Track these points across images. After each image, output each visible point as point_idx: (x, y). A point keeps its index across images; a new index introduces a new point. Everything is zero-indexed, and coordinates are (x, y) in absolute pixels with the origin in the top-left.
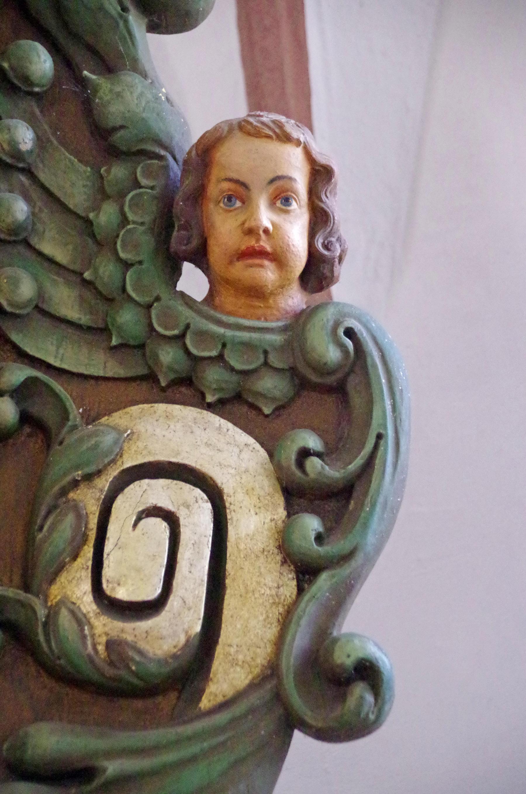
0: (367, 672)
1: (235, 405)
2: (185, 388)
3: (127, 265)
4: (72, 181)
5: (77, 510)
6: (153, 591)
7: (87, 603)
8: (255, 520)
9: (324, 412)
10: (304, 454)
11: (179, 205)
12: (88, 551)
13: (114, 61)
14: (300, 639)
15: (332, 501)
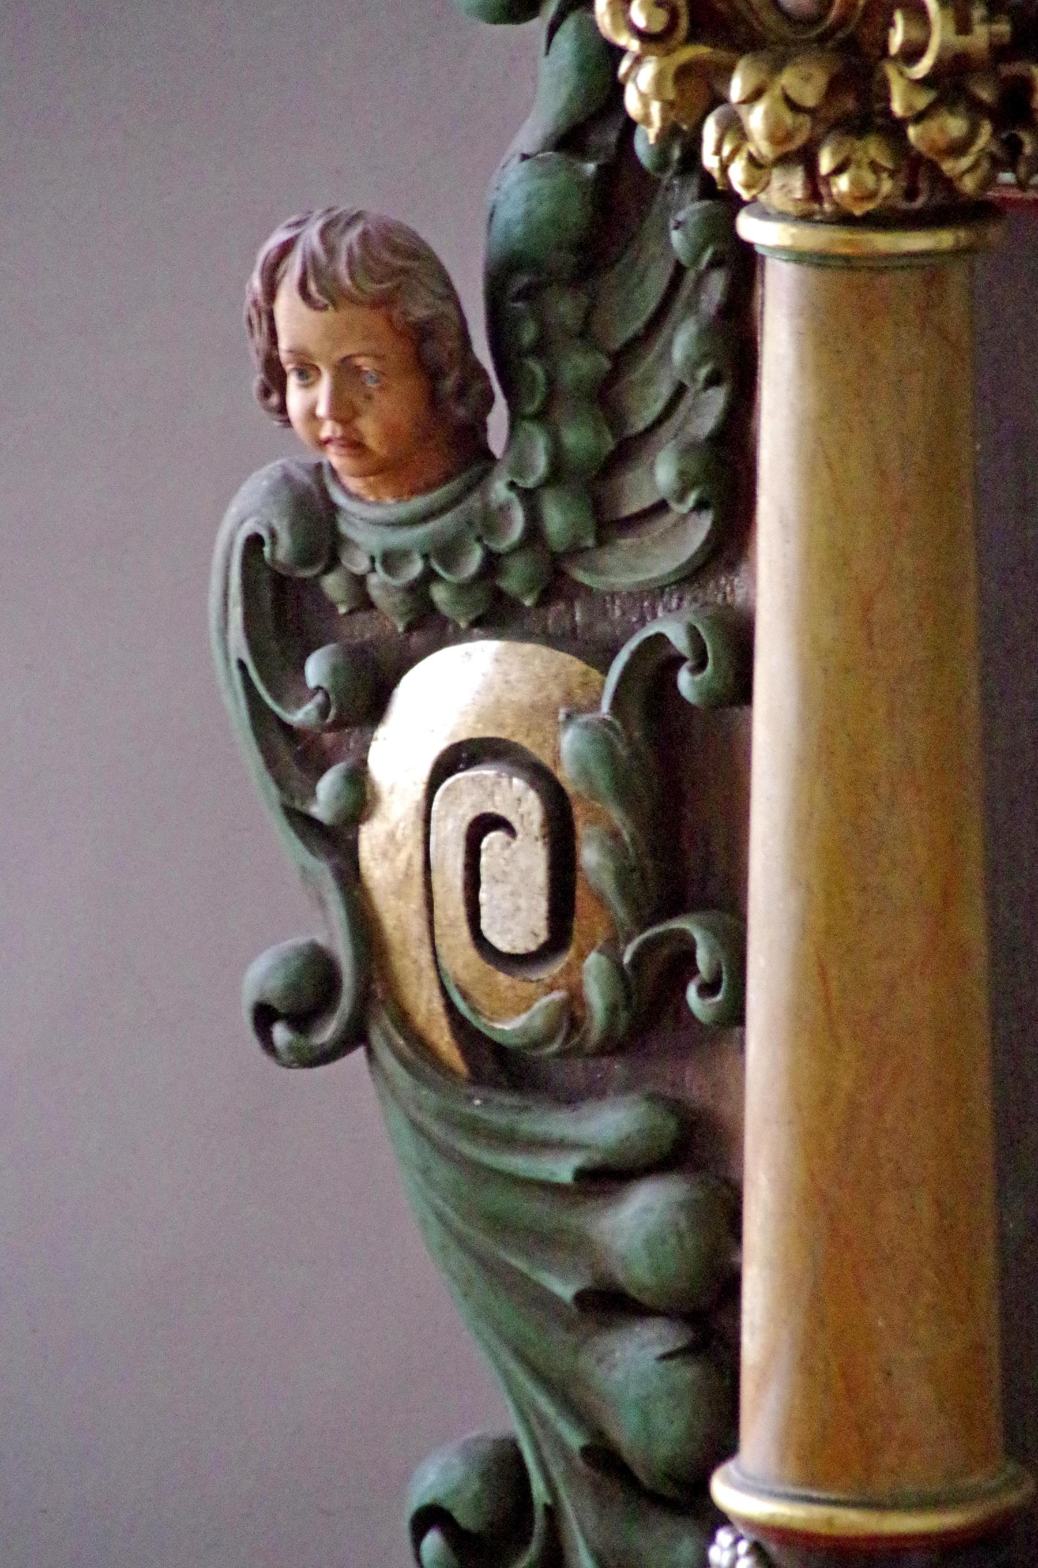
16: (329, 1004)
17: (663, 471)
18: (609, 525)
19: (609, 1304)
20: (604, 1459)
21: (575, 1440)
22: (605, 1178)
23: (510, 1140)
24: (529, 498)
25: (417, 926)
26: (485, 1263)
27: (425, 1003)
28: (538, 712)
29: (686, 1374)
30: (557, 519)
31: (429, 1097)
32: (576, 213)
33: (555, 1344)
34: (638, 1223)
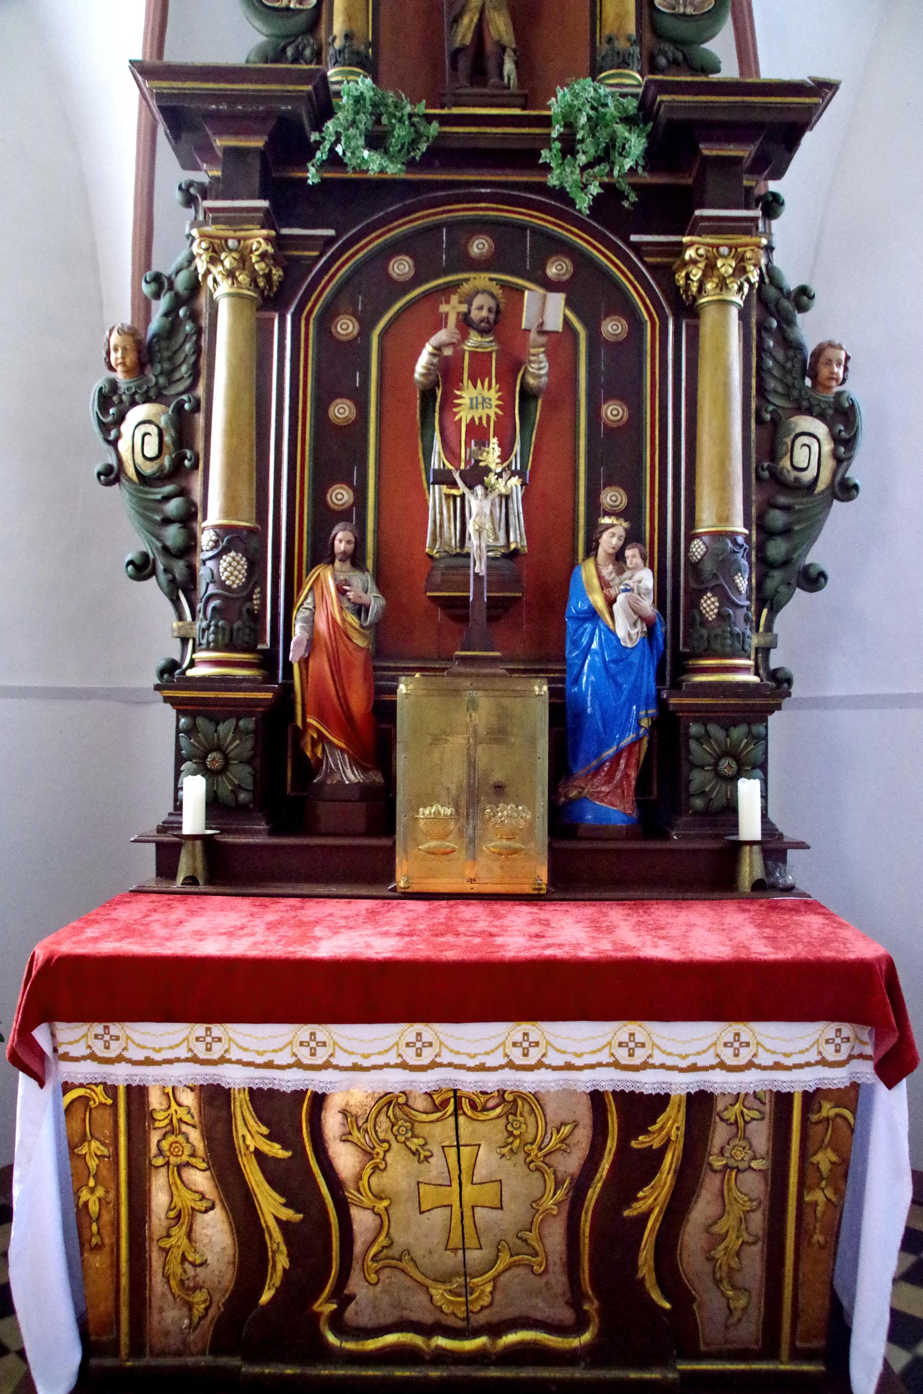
0: (856, 487)
1: (822, 417)
2: (809, 412)
3: (795, 378)
4: (780, 355)
5: (786, 443)
6: (805, 465)
7: (789, 467)
8: (827, 447)
9: (843, 419)
10: (840, 431)
12: (789, 455)
13: (791, 322)
14: (838, 478)
15: (845, 443)
16: (111, 475)
18: (171, 382)
19: (167, 521)
20: (166, 549)
21: (159, 545)
22: (167, 498)
23: (147, 493)
24: (156, 377)
25: (130, 457)
26: (142, 515)
27: (131, 471)
28: (158, 415)
29: (182, 531)
30: (162, 380)
31: (133, 486)
32: (168, 326)
33: (156, 530)
34: (173, 507)
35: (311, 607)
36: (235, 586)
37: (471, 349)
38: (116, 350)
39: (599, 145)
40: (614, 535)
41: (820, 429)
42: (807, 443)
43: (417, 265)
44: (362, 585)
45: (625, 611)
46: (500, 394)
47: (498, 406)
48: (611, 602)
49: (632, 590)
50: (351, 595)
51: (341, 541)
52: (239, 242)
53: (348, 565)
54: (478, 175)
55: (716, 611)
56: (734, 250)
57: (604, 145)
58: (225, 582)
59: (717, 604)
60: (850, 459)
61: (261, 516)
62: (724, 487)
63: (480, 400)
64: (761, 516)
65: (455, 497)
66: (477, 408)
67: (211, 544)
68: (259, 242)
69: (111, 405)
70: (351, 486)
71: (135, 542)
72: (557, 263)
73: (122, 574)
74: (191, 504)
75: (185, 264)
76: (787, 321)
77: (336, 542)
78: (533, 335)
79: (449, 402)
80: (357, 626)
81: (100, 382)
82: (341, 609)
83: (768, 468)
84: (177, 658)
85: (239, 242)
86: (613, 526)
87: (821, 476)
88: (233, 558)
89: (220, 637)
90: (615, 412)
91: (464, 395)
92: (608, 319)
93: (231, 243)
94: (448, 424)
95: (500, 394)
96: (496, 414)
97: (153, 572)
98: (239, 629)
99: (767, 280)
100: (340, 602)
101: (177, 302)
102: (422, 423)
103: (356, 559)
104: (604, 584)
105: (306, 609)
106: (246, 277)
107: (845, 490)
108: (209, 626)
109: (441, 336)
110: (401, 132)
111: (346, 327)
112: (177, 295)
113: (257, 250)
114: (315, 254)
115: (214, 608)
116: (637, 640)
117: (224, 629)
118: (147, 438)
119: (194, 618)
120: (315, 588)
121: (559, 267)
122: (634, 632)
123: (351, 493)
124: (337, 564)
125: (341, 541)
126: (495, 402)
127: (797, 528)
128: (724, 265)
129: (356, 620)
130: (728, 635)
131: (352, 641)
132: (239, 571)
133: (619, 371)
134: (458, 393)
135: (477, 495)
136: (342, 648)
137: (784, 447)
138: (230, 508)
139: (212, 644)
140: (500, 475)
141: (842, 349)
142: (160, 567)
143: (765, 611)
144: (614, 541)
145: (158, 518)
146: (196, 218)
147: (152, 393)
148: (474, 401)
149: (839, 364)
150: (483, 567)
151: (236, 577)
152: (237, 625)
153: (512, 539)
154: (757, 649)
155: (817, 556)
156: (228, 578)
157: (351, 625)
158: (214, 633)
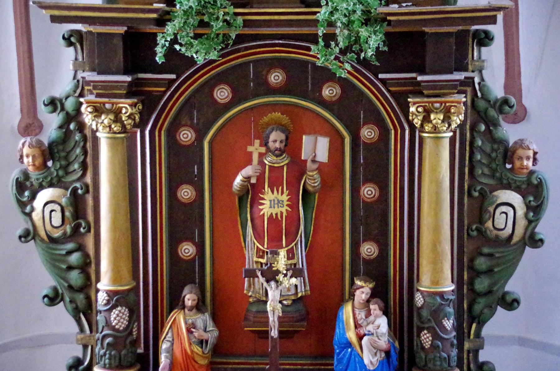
1: (518, 190)
2: (508, 187)
3: (497, 165)
5: (490, 212)
6: (503, 227)
8: (521, 211)
9: (534, 192)
11: (508, 153)
12: (491, 219)
13: (496, 124)
15: (535, 209)
17: (76, 166)
18: (67, 173)
19: (70, 268)
20: (70, 287)
21: (66, 285)
22: (69, 253)
23: (56, 249)
24: (57, 170)
25: (42, 224)
27: (42, 234)
28: (60, 197)
29: (81, 275)
30: (61, 173)
31: (44, 245)
33: (63, 275)
34: (75, 258)
35: (171, 339)
36: (121, 328)
37: (270, 164)
38: (28, 156)
39: (351, 38)
40: (363, 292)
41: (515, 198)
42: (506, 211)
43: (234, 91)
44: (203, 320)
45: (368, 348)
46: (289, 197)
47: (287, 205)
48: (360, 338)
49: (373, 334)
50: (196, 334)
51: (189, 300)
52: (113, 105)
53: (194, 311)
54: (271, 66)
55: (430, 343)
56: (443, 104)
57: (354, 38)
58: (115, 326)
59: (431, 338)
60: (538, 220)
61: (135, 277)
62: (436, 262)
63: (276, 202)
64: (472, 260)
65: (262, 264)
66: (274, 207)
67: (105, 302)
68: (126, 108)
69: (25, 188)
70: (194, 244)
71: (47, 281)
72: (330, 88)
73: (40, 305)
74: (86, 256)
75: (72, 93)
76: (492, 124)
77: (186, 300)
78: (309, 164)
79: (256, 201)
80: (201, 353)
81: (15, 174)
82: (190, 344)
83: (477, 229)
84: (80, 355)
85: (113, 105)
86: (362, 287)
87: (516, 231)
88: (120, 311)
89: (113, 362)
90: (370, 193)
91: (265, 198)
92: (366, 127)
93: (108, 106)
94: (256, 216)
95: (289, 197)
96: (287, 210)
97: (62, 299)
98: (125, 355)
99: (479, 94)
100: (189, 339)
101: (69, 119)
102: (239, 206)
103: (199, 307)
104: (357, 326)
105: (167, 341)
106: (118, 128)
107: (534, 241)
108: (105, 354)
109: (248, 171)
110: (217, 26)
111: (186, 136)
112: (67, 113)
113: (126, 113)
114: (163, 89)
115: (108, 344)
116: (376, 364)
117: (115, 357)
118: (53, 213)
119: (91, 331)
120: (173, 326)
121: (330, 92)
122: (374, 360)
123: (195, 248)
124: (186, 310)
125: (189, 300)
126: (286, 203)
127: (496, 270)
128: (435, 119)
129: (200, 349)
130: (438, 359)
131: (197, 363)
132: (124, 319)
133: (373, 163)
134: (262, 196)
135: (272, 287)
136: (191, 367)
137: (488, 215)
138: (116, 279)
139: (107, 366)
140: (286, 275)
141: (530, 149)
142: (67, 299)
143: (474, 326)
144: (364, 296)
145: (64, 267)
146: (76, 59)
147: (55, 181)
148: (273, 202)
149: (528, 158)
150: (276, 332)
151: (122, 323)
152: (123, 352)
153: (299, 290)
154: (469, 352)
155: (513, 286)
156: (117, 324)
157: (197, 354)
158: (110, 359)
